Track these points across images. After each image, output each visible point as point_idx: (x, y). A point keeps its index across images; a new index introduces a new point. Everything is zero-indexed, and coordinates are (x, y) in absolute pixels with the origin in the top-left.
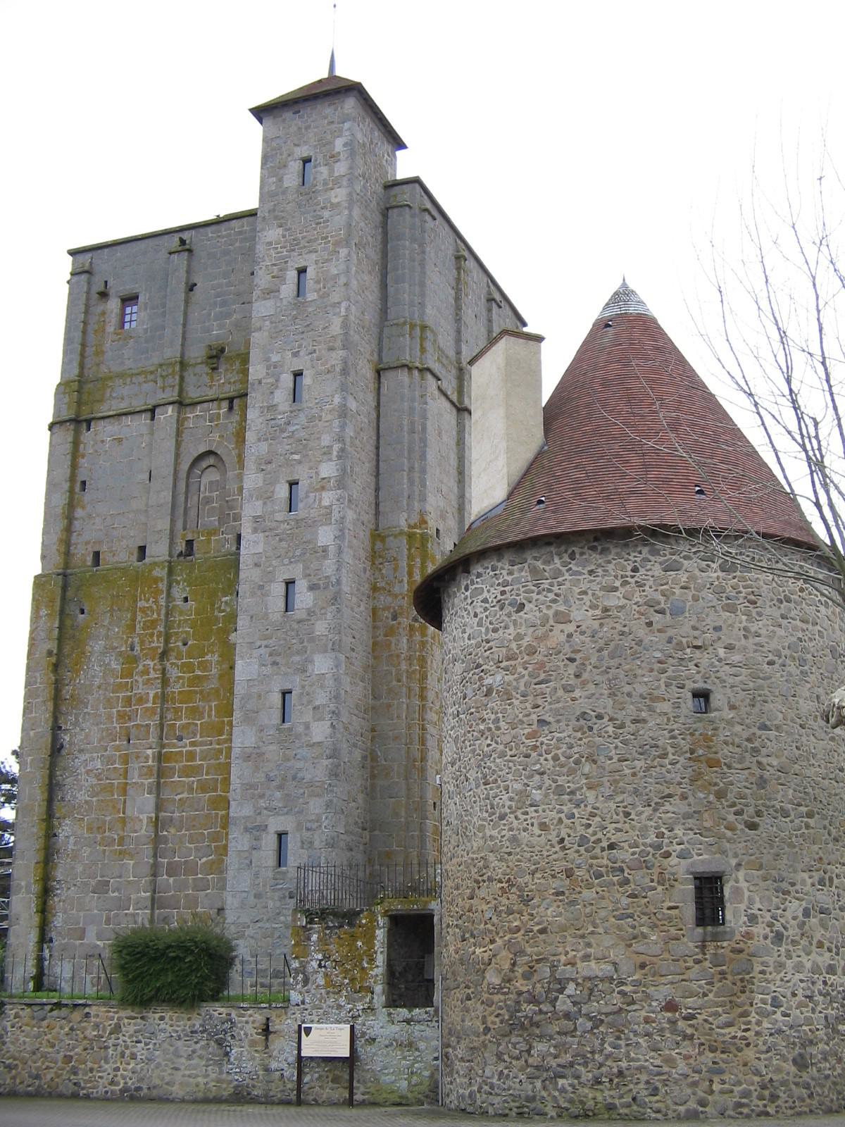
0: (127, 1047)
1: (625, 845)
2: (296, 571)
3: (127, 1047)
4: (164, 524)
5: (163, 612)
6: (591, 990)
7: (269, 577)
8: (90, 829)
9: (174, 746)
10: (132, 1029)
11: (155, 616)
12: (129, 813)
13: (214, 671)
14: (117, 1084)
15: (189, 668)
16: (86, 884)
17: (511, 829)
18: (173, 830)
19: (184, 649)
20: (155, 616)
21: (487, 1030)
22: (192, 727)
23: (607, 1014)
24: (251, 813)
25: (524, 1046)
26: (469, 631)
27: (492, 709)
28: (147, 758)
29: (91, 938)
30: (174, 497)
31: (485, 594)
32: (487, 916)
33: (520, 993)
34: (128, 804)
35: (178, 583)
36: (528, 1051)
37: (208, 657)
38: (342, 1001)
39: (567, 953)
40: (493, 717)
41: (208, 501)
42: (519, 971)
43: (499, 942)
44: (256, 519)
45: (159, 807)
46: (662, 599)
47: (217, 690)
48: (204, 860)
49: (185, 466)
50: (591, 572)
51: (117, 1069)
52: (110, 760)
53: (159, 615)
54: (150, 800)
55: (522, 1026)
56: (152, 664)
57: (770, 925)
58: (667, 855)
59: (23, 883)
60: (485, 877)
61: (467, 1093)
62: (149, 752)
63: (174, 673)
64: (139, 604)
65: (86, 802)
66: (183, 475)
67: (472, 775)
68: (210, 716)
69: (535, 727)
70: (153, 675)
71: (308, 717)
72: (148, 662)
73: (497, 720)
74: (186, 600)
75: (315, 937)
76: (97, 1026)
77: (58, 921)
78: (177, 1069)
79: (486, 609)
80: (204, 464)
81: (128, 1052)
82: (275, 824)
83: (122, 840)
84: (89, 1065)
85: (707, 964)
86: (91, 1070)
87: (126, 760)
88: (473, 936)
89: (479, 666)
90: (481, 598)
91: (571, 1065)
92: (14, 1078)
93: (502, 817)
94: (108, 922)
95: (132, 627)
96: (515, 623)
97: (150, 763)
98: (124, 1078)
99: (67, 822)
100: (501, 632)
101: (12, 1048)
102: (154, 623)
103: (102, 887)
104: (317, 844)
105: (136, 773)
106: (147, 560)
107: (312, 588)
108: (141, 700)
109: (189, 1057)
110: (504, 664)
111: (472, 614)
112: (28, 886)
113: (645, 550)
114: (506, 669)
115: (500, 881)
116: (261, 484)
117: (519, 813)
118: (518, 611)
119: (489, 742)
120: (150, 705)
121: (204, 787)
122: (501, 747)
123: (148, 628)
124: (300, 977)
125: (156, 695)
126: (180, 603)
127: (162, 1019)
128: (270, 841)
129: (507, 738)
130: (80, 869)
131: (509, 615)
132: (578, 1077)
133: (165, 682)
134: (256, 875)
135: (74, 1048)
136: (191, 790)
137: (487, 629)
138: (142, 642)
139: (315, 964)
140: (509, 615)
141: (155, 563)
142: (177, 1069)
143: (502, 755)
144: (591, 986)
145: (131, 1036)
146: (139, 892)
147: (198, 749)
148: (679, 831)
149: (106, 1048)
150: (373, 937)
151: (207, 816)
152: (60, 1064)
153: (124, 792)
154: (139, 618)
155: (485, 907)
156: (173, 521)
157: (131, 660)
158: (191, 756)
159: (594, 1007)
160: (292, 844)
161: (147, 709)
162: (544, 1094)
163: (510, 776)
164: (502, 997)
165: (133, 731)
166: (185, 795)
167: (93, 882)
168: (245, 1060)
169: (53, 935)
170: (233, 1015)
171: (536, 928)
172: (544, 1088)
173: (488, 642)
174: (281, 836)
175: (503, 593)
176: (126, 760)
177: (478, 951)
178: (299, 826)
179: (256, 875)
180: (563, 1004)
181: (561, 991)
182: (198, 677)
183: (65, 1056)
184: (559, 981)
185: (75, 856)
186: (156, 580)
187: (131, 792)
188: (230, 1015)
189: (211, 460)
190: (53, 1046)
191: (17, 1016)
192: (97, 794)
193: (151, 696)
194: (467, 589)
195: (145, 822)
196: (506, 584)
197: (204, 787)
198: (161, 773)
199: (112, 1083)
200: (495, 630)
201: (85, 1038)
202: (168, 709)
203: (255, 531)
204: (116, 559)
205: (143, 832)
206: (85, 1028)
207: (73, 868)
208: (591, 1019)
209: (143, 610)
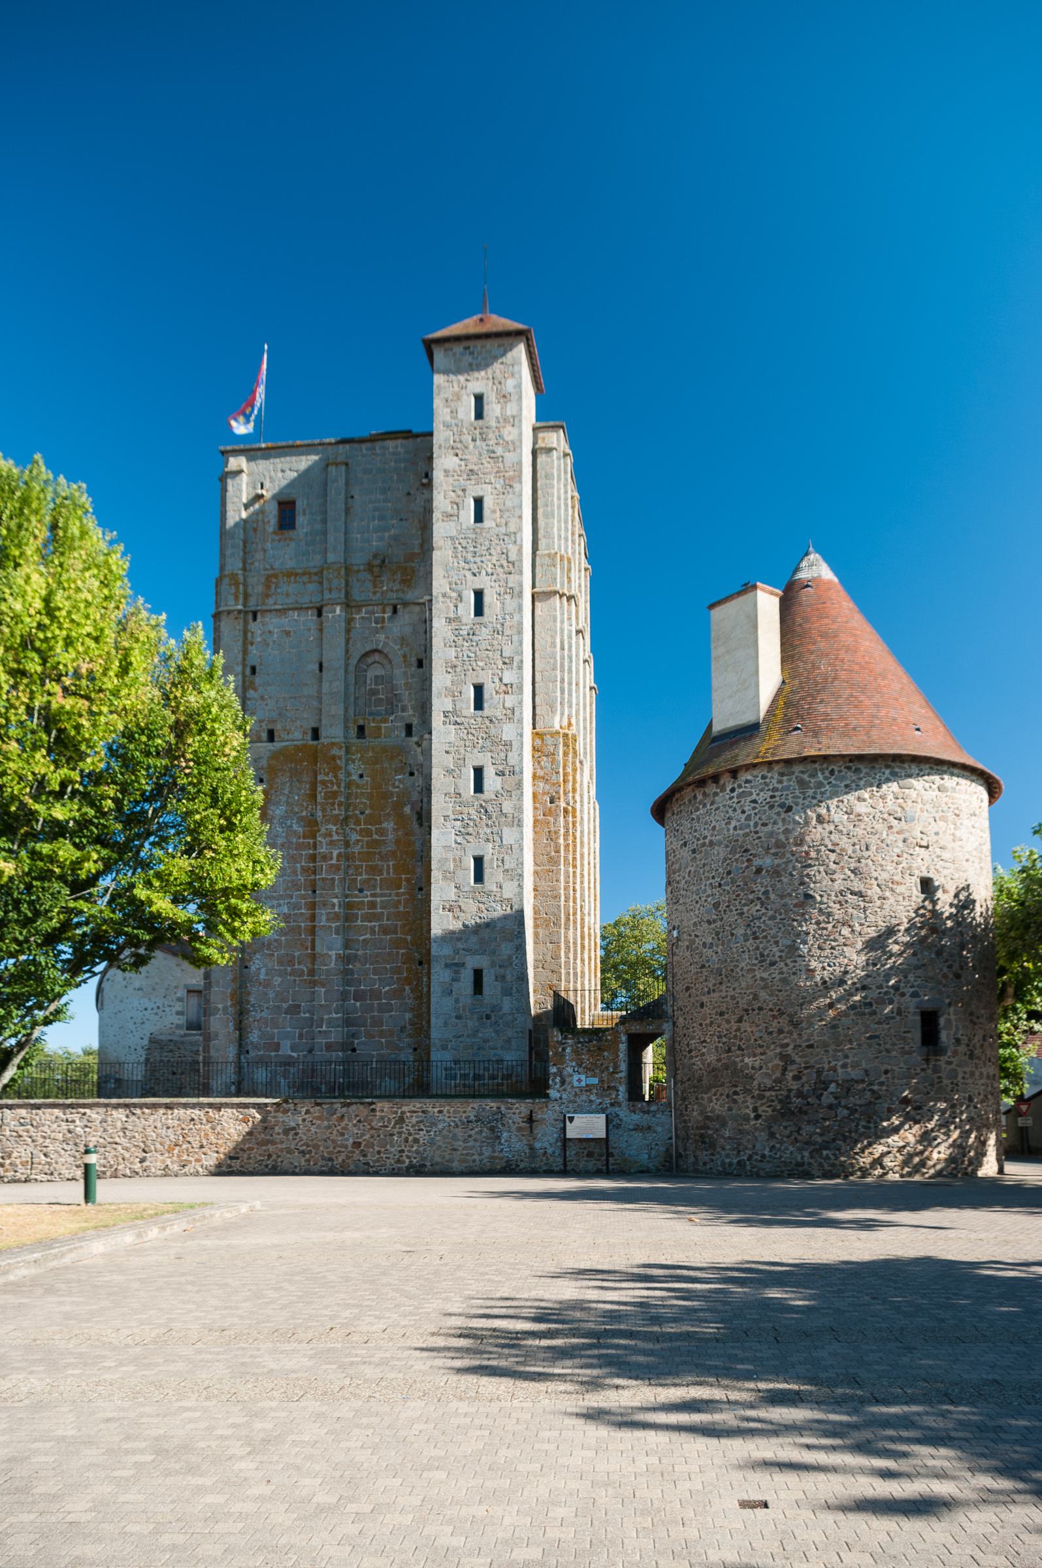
0: (410, 1134)
1: (874, 987)
2: (484, 760)
3: (410, 1134)
4: (338, 710)
5: (343, 785)
6: (849, 1090)
7: (461, 762)
8: (280, 963)
9: (356, 896)
10: (414, 1120)
11: (335, 788)
12: (318, 949)
13: (390, 837)
14: (404, 1162)
15: (368, 833)
16: (278, 1007)
17: (782, 973)
18: (358, 965)
19: (362, 817)
20: (335, 788)
21: (757, 1117)
22: (372, 882)
23: (860, 1106)
24: (451, 953)
25: (794, 1129)
26: (734, 823)
27: (761, 883)
28: (333, 905)
29: (286, 1050)
30: (346, 687)
31: (754, 797)
32: (757, 1035)
33: (790, 1091)
34: (317, 942)
35: (353, 761)
36: (798, 1132)
37: (385, 825)
38: (593, 1097)
39: (829, 1062)
40: (763, 890)
41: (374, 692)
42: (790, 1075)
43: (770, 1053)
44: (446, 714)
45: (347, 945)
46: (899, 810)
47: (394, 853)
48: (387, 988)
49: (354, 661)
50: (847, 786)
51: (402, 1151)
52: (296, 906)
53: (339, 786)
54: (338, 940)
55: (793, 1113)
56: (334, 828)
57: (968, 1045)
58: (903, 995)
59: (220, 1006)
60: (756, 1007)
61: (735, 1161)
62: (335, 901)
63: (354, 837)
64: (319, 778)
65: (276, 940)
66: (352, 668)
67: (740, 932)
68: (388, 873)
69: (802, 898)
70: (335, 837)
71: (500, 877)
72: (330, 826)
73: (766, 893)
74: (361, 776)
75: (568, 1050)
76: (382, 1118)
77: (254, 1037)
78: (455, 1150)
79: (754, 808)
80: (370, 660)
81: (411, 1138)
82: (472, 962)
83: (312, 972)
84: (377, 1149)
85: (929, 1071)
86: (379, 1153)
87: (313, 906)
88: (740, 1048)
89: (746, 851)
90: (749, 799)
91: (834, 1140)
92: (308, 1161)
93: (773, 964)
94: (301, 1036)
95: (313, 796)
96: (784, 820)
97: (337, 909)
98: (408, 1157)
99: (258, 956)
100: (770, 826)
101: (304, 1138)
102: (335, 795)
103: (295, 1009)
104: (509, 978)
105: (324, 918)
106: (322, 740)
107: (500, 774)
108: (325, 858)
109: (465, 1141)
110: (773, 851)
111: (739, 811)
112: (225, 1009)
113: (887, 772)
114: (775, 854)
115: (771, 1010)
116: (449, 684)
117: (788, 961)
118: (786, 812)
119: (758, 907)
120: (334, 862)
121: (385, 930)
122: (771, 913)
123: (330, 798)
124: (558, 1080)
125: (339, 855)
126: (355, 777)
127: (440, 1112)
128: (467, 977)
129: (777, 906)
130: (272, 995)
131: (778, 814)
132: (839, 1150)
133: (347, 844)
134: (457, 1001)
135: (363, 1135)
136: (373, 932)
137: (756, 824)
138: (324, 810)
139: (569, 1070)
140: (778, 814)
141: (333, 744)
142: (455, 1150)
143: (772, 918)
144: (848, 1087)
145: (413, 1126)
146: (330, 1013)
147: (378, 900)
148: (911, 977)
149: (392, 1135)
150: (618, 1050)
151: (389, 954)
152: (350, 1148)
153: (312, 931)
154: (319, 789)
155: (755, 1029)
156: (346, 709)
157: (312, 825)
158: (373, 905)
159: (853, 1101)
160: (487, 979)
161: (332, 866)
162: (812, 1161)
163: (780, 934)
164: (774, 1093)
165: (319, 883)
166: (368, 936)
167: (285, 1006)
168: (513, 1143)
169: (250, 1048)
170: (503, 1108)
171: (804, 1045)
172: (812, 1157)
173: (756, 832)
174: (478, 974)
175: (772, 797)
176: (313, 906)
177: (746, 1060)
178: (493, 964)
179: (457, 1001)
180: (827, 1099)
181: (826, 1089)
182: (377, 841)
183: (354, 1143)
184: (824, 1083)
185: (267, 984)
186: (334, 758)
187: (319, 932)
188: (499, 1108)
189: (377, 657)
190: (342, 1134)
191: (307, 1112)
192: (285, 934)
193: (335, 855)
194: (733, 790)
195: (334, 957)
196: (775, 790)
197: (385, 930)
198: (348, 918)
199: (398, 1161)
200: (764, 825)
201: (372, 1128)
202: (349, 866)
203: (444, 723)
204: (291, 736)
205: (332, 965)
206: (372, 1121)
207: (266, 994)
208: (848, 1109)
209: (323, 783)
